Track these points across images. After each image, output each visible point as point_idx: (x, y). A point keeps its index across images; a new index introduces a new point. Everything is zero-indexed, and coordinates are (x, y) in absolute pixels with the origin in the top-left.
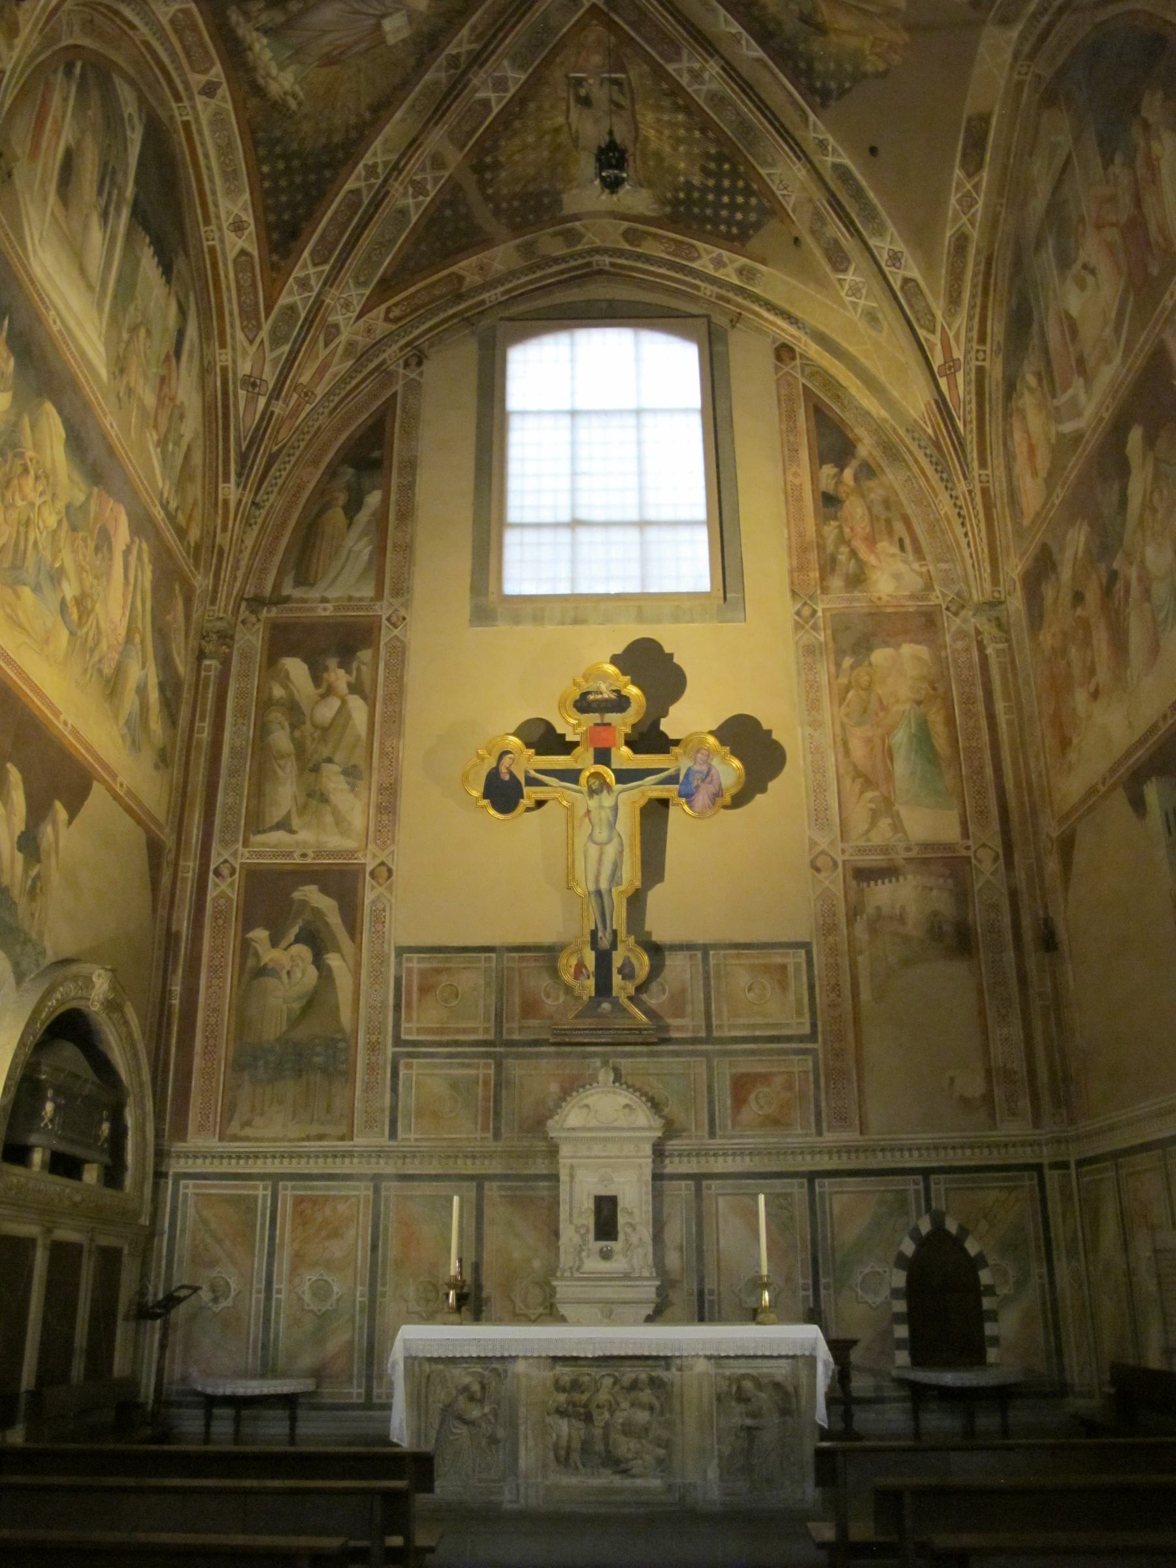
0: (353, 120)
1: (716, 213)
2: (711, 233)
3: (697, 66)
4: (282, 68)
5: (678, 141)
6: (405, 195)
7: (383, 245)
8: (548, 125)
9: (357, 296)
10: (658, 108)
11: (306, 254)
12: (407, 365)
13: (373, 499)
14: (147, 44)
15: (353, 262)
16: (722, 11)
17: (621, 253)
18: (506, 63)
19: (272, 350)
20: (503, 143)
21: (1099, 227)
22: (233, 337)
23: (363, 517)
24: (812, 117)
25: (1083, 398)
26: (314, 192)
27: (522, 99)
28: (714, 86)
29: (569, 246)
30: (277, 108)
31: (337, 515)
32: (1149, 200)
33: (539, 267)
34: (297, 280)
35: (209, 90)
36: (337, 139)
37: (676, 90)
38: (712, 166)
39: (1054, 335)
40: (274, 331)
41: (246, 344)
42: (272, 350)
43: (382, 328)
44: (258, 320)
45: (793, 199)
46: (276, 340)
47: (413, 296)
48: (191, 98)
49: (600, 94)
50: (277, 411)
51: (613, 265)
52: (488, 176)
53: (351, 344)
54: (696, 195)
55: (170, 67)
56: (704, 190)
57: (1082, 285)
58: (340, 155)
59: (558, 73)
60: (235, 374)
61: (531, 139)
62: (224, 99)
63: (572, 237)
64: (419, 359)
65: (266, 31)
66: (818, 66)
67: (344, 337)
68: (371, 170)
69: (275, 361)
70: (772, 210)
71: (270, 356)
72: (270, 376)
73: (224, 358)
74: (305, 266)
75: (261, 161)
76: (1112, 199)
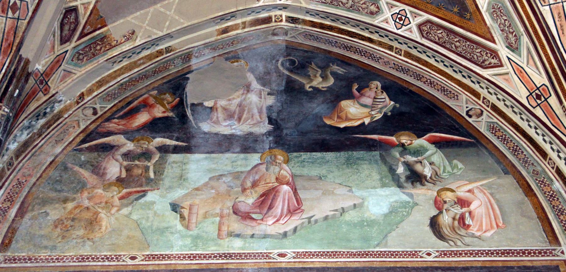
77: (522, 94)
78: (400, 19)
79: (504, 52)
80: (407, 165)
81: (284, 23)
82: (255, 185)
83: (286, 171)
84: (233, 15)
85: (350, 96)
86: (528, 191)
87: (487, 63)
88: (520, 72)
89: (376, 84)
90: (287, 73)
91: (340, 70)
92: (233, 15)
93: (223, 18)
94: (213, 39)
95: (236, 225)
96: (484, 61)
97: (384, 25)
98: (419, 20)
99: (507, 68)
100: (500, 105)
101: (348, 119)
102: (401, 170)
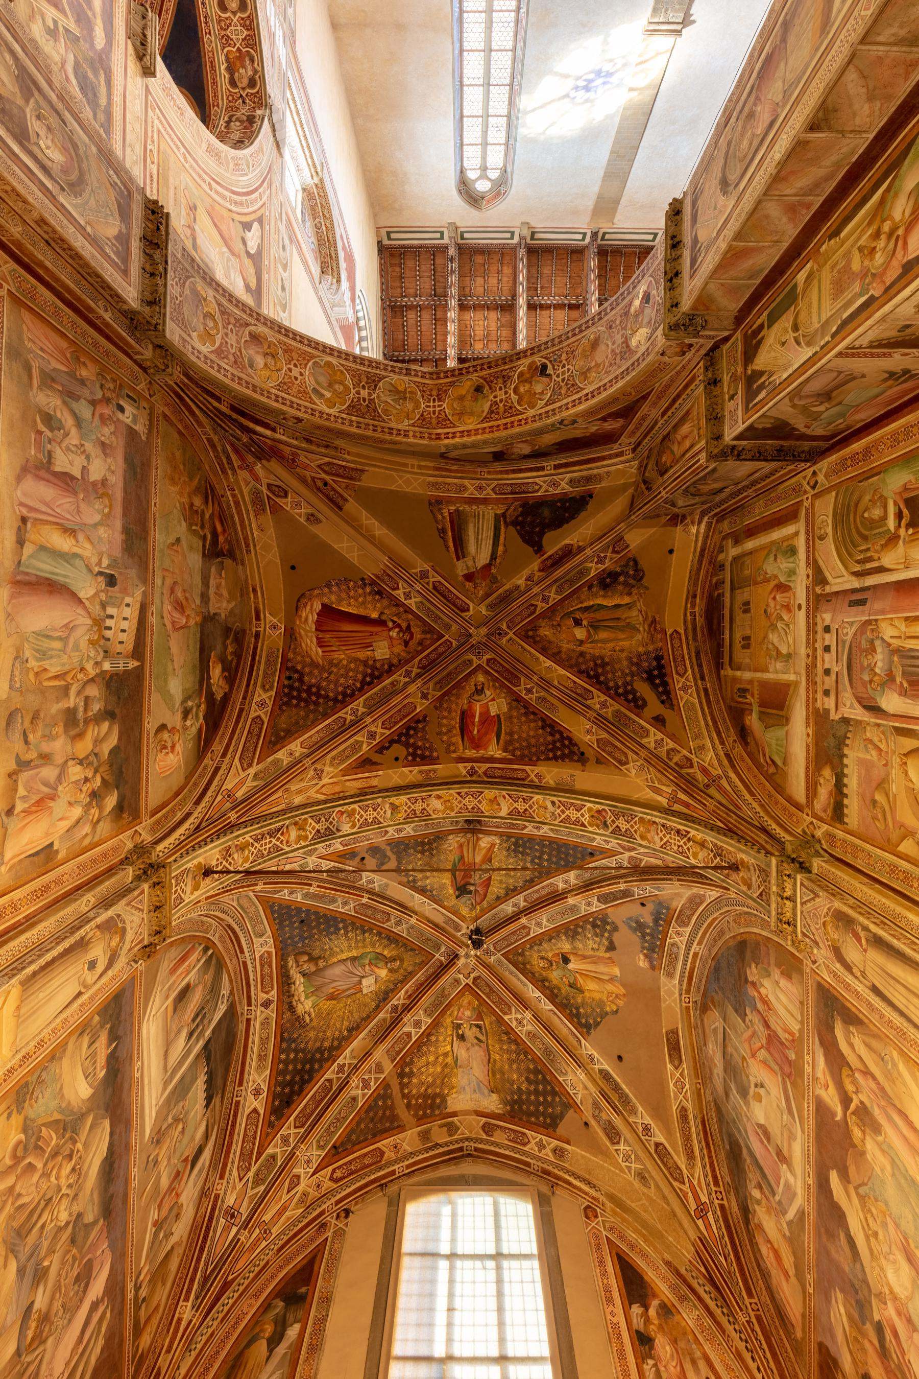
0: (337, 1035)
1: (537, 1110)
2: (535, 1124)
3: (520, 1016)
4: (307, 998)
5: (511, 1062)
6: (357, 1087)
7: (339, 1120)
8: (441, 1050)
9: (316, 1155)
10: (500, 1041)
11: (292, 1118)
12: (338, 1217)
13: (293, 1332)
14: (245, 963)
15: (320, 1128)
16: (530, 985)
17: (481, 1141)
18: (421, 1012)
19: (252, 1188)
20: (416, 1060)
21: (753, 1055)
22: (230, 1173)
23: (281, 1349)
24: (583, 1041)
25: (791, 1180)
26: (306, 1077)
27: (428, 1034)
28: (530, 1028)
29: (450, 1136)
30: (299, 1020)
31: (262, 1346)
32: (772, 1024)
33: (431, 1148)
34: (282, 1136)
35: (266, 1004)
36: (327, 1044)
37: (509, 1031)
38: (532, 1077)
39: (756, 1147)
40: (257, 1174)
41: (237, 1180)
42: (252, 1188)
43: (328, 1184)
44: (250, 1164)
45: (580, 1096)
46: (257, 1182)
47: (350, 1162)
48: (256, 1006)
49: (470, 1033)
50: (242, 1238)
51: (476, 1149)
52: (406, 1080)
53: (305, 1195)
54: (524, 1097)
55: (252, 983)
56: (529, 1093)
57: (759, 1098)
58: (326, 1055)
59: (448, 1020)
60: (223, 1201)
61: (432, 1059)
62: (272, 1011)
63: (452, 1129)
64: (347, 1212)
65: (304, 975)
66: (581, 1010)
67: (300, 1188)
68: (341, 1068)
69: (252, 1198)
70: (569, 1104)
71: (250, 1193)
72: (245, 1211)
73: (220, 1187)
74: (289, 1128)
75: (282, 1051)
76: (754, 1034)
78: (262, 704)
79: (252, 771)
80: (192, 708)
82: (186, 599)
83: (192, 622)
85: (223, 670)
86: (177, 794)
95: (169, 582)
97: (257, 694)
98: (263, 716)
99: (243, 775)
102: (190, 703)
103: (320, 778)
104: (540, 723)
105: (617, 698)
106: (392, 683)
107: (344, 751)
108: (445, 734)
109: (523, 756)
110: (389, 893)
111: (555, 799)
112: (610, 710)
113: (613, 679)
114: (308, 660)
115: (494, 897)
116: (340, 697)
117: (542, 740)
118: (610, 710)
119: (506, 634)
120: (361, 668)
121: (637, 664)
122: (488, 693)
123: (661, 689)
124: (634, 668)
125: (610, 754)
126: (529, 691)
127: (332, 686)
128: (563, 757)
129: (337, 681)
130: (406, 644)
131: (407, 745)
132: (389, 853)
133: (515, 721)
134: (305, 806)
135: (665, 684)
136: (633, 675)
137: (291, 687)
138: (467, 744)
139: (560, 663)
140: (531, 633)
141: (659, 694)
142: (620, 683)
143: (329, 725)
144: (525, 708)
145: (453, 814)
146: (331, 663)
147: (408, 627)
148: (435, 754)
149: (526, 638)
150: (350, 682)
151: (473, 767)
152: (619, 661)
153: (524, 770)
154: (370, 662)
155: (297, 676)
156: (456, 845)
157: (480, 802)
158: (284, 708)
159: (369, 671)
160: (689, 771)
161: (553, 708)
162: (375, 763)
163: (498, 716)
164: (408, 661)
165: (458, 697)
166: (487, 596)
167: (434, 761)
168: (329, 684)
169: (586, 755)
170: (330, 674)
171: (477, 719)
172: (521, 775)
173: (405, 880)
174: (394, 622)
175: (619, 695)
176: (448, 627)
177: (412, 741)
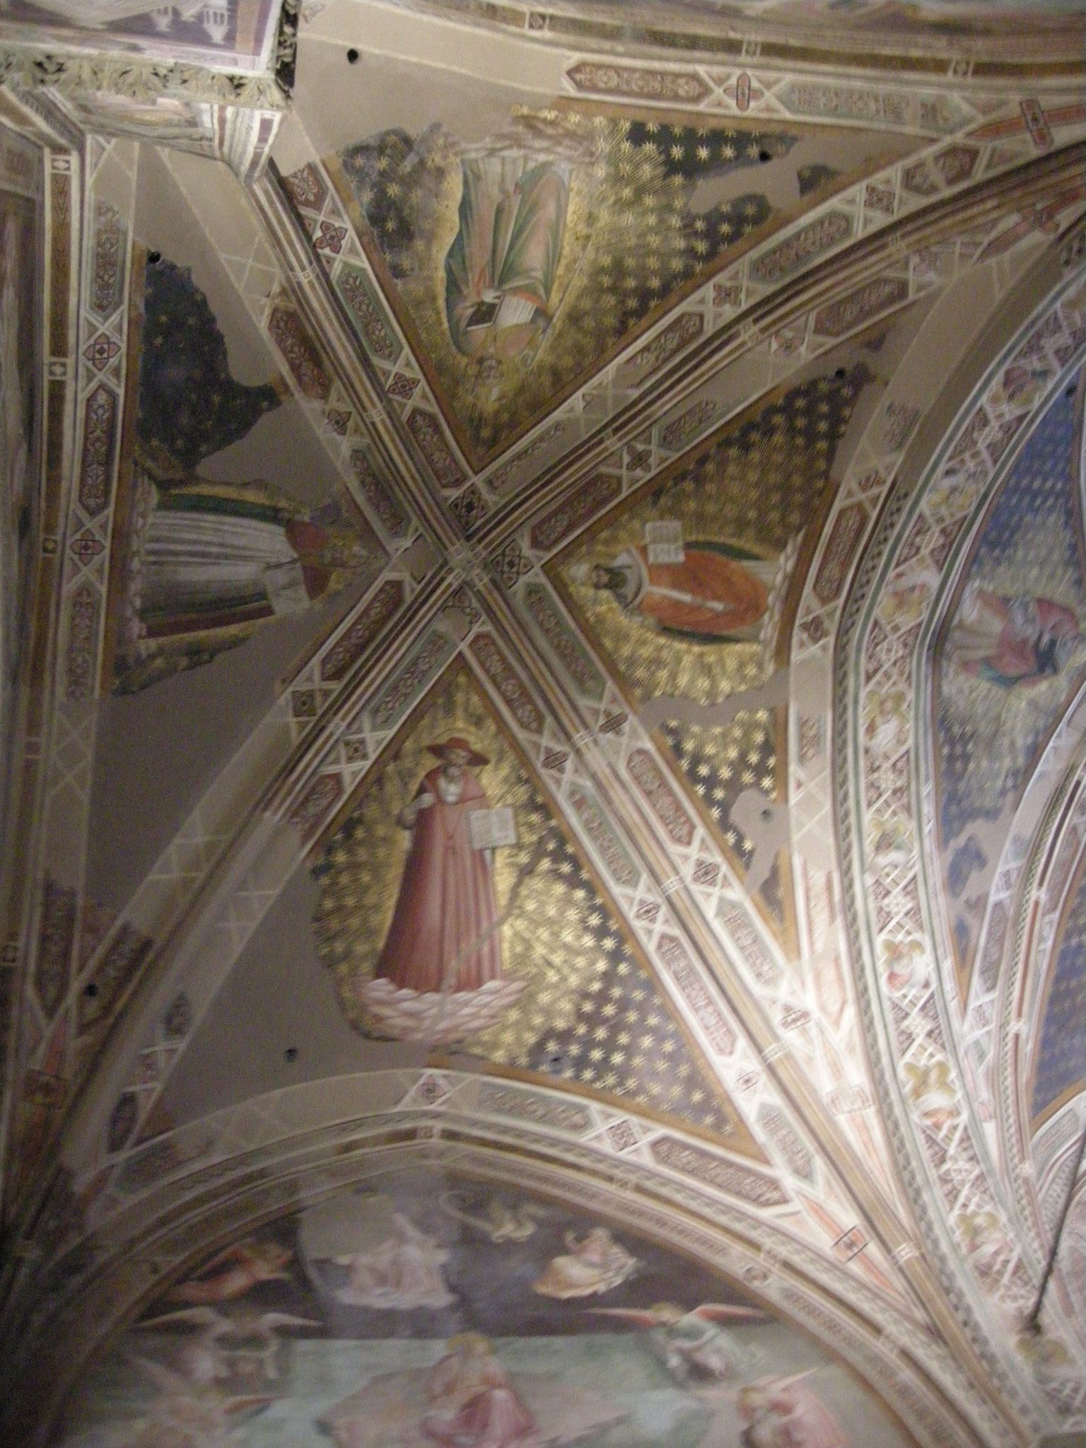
77: (825, 1242)
79: (790, 1182)
81: (434, 1140)
84: (360, 1124)
85: (564, 1251)
87: (763, 1199)
88: (818, 1210)
89: (600, 1234)
90: (458, 1215)
91: (541, 1212)
92: (360, 1124)
93: (343, 1128)
94: (327, 1161)
96: (760, 1196)
100: (797, 1260)
101: (571, 1286)
103: (805, 1015)
104: (733, 452)
105: (718, 261)
106: (579, 804)
107: (742, 949)
108: (714, 685)
109: (806, 507)
110: (1028, 831)
111: (942, 468)
112: (745, 283)
113: (664, 256)
114: (514, 1015)
115: (1073, 591)
116: (609, 944)
117: (778, 458)
118: (745, 283)
119: (473, 491)
120: (537, 884)
121: (640, 192)
122: (622, 560)
123: (729, 152)
124: (649, 201)
125: (863, 315)
126: (640, 460)
127: (580, 962)
128: (836, 420)
129: (566, 947)
130: (479, 760)
131: (734, 787)
132: (959, 842)
133: (711, 508)
134: (873, 1062)
135: (717, 138)
136: (669, 209)
137: (581, 1063)
138: (745, 630)
139: (582, 374)
140: (486, 433)
141: (741, 159)
142: (680, 244)
143: (677, 978)
144: (683, 477)
145: (911, 695)
146: (523, 958)
147: (437, 750)
148: (762, 715)
149: (495, 444)
150: (572, 915)
151: (805, 627)
152: (616, 231)
153: (842, 513)
154: (524, 858)
155: (552, 1047)
156: (962, 677)
157: (896, 629)
158: (631, 1083)
159: (545, 864)
160: (983, 160)
161: (701, 414)
162: (775, 871)
163: (688, 546)
164: (523, 760)
165: (622, 637)
166: (367, 533)
167: (778, 724)
168: (574, 969)
169: (849, 368)
170: (549, 964)
171: (686, 598)
172: (852, 521)
173: (1010, 796)
174: (422, 790)
175: (711, 254)
176: (438, 643)
177: (725, 773)
